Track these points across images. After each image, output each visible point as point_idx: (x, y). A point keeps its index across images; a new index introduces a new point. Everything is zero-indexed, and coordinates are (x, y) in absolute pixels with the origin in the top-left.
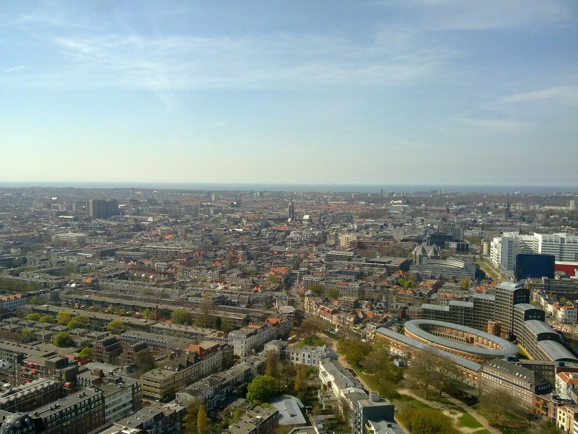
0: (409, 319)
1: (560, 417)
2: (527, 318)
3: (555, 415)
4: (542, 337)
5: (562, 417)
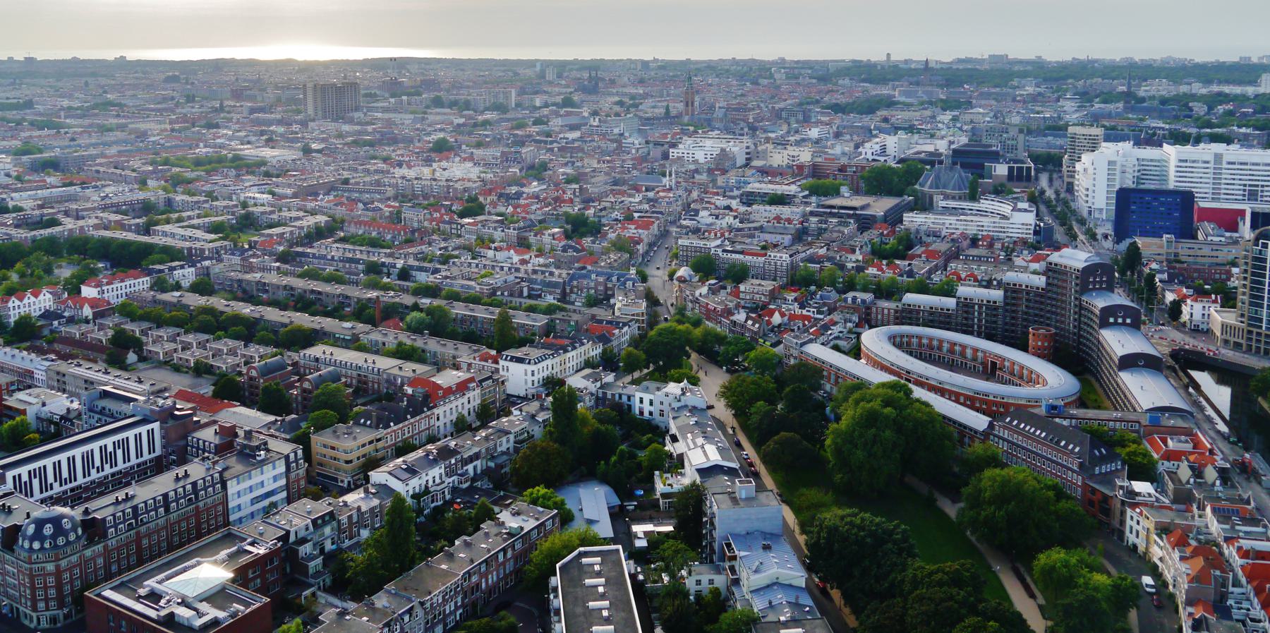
0: (871, 327)
1: (1131, 528)
2: (1104, 324)
3: (1123, 522)
4: (1130, 362)
5: (1136, 527)
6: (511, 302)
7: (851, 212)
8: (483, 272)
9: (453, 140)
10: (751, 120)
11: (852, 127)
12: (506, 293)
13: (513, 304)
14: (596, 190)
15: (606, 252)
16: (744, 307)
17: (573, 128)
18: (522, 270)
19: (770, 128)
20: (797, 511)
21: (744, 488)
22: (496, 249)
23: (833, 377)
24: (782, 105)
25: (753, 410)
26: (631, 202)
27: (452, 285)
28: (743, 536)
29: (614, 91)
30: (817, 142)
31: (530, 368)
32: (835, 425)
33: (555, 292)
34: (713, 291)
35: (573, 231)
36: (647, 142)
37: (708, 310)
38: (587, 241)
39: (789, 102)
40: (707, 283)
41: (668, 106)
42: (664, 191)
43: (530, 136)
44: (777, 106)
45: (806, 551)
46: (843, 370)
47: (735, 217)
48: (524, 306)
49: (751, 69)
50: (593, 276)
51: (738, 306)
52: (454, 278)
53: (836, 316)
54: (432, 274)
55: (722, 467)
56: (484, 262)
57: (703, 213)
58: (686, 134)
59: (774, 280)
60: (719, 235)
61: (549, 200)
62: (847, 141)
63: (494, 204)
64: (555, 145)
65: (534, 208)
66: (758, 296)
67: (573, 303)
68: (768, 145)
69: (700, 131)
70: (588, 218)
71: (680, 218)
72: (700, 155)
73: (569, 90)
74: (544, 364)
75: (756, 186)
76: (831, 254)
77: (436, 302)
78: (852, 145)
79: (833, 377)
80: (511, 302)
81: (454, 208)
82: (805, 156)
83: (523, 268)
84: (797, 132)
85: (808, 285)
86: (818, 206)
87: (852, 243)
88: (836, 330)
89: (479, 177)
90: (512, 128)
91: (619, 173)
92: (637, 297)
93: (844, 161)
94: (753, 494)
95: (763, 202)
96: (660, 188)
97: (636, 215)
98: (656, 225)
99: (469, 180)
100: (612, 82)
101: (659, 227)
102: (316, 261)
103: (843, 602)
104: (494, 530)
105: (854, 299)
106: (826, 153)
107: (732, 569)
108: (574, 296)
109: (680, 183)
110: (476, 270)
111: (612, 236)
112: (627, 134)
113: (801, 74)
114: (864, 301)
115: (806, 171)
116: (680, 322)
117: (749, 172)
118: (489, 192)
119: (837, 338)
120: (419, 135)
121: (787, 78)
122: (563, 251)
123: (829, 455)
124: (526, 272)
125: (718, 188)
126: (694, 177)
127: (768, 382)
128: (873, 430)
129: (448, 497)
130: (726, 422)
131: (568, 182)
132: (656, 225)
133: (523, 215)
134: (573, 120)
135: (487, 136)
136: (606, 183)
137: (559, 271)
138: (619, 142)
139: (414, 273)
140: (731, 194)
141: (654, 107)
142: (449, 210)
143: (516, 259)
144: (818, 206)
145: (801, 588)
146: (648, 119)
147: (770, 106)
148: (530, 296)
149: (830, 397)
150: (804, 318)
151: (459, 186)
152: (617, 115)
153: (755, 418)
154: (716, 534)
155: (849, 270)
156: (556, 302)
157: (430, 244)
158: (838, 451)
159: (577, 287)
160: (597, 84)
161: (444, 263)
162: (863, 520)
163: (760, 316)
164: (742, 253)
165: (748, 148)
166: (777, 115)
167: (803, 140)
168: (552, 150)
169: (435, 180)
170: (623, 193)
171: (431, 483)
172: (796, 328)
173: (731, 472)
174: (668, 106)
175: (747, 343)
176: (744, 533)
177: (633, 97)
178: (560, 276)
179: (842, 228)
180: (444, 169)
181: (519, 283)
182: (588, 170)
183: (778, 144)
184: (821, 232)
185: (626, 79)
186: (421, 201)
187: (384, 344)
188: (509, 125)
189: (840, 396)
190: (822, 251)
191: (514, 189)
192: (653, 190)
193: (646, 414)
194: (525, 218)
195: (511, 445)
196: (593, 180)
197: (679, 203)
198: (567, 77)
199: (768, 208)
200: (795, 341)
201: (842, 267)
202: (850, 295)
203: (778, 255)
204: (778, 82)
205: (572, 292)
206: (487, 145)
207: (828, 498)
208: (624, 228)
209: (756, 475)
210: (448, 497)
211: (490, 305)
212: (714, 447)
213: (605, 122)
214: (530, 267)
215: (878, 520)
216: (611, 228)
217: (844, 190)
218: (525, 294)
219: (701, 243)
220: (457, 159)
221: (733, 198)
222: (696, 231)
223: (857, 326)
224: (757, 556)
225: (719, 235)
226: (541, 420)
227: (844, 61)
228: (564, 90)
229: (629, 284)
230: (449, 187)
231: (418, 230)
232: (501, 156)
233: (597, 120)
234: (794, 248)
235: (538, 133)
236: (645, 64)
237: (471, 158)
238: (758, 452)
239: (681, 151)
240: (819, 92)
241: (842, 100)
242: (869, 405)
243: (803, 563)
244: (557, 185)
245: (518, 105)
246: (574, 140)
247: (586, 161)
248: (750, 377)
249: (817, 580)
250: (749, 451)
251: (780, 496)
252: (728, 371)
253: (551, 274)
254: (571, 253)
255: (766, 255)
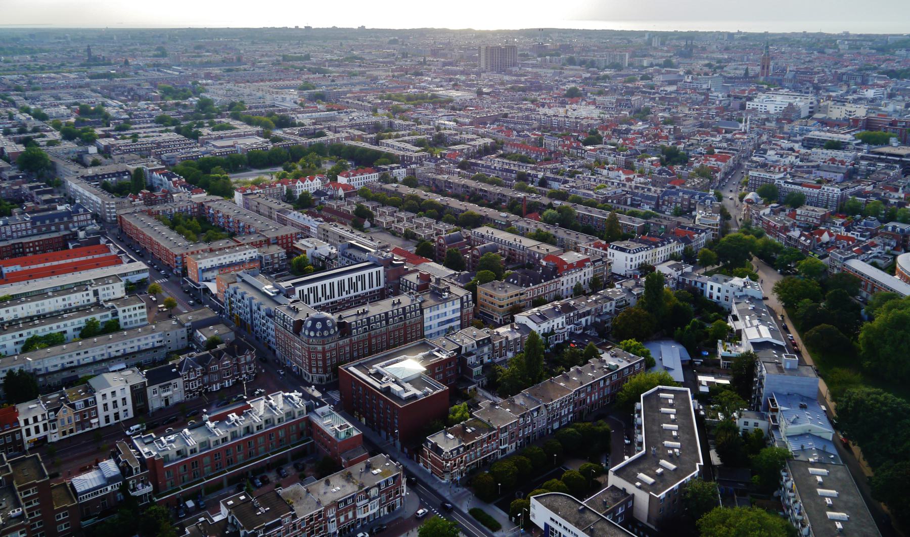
6: (618, 208)
7: (898, 159)
8: (599, 185)
9: (581, 89)
10: (816, 81)
11: (905, 89)
12: (615, 201)
13: (620, 210)
14: (686, 130)
15: (692, 177)
16: (798, 227)
17: (671, 83)
18: (628, 186)
19: (832, 88)
20: (829, 384)
21: (788, 360)
22: (609, 169)
23: (869, 287)
24: (843, 70)
25: (800, 304)
26: (713, 141)
27: (576, 193)
28: (785, 395)
29: (705, 56)
30: (873, 100)
31: (630, 256)
32: (869, 324)
33: (651, 203)
34: (774, 212)
35: (667, 160)
36: (729, 96)
37: (770, 226)
38: (677, 168)
39: (849, 68)
40: (770, 206)
41: (747, 69)
42: (739, 134)
43: (638, 88)
44: (839, 71)
45: (835, 415)
46: (879, 282)
47: (797, 157)
48: (627, 211)
49: (819, 40)
50: (681, 194)
51: (793, 225)
52: (578, 188)
53: (876, 240)
54: (563, 184)
55: (772, 343)
56: (600, 178)
57: (770, 152)
58: (760, 91)
59: (826, 207)
60: (782, 170)
61: (650, 136)
62: (898, 101)
63: (609, 137)
64: (657, 95)
65: (638, 141)
66: (811, 219)
67: (664, 212)
68: (829, 102)
69: (772, 89)
70: (679, 151)
71: (751, 155)
72: (771, 108)
73: (669, 54)
74: (640, 254)
75: (815, 134)
76: (876, 191)
77: (565, 204)
78: (903, 104)
79: (869, 287)
80: (618, 208)
81: (580, 138)
82: (861, 112)
83: (628, 184)
84: (855, 92)
85: (854, 214)
86: (869, 152)
87: (896, 183)
88: (875, 251)
89: (599, 117)
90: (625, 82)
91: (705, 118)
92: (713, 212)
93: (895, 117)
94: (796, 366)
95: (822, 147)
96: (737, 132)
97: (716, 151)
98: (731, 159)
99: (592, 119)
100: (704, 49)
101: (734, 161)
102: (483, 169)
103: (862, 457)
104: (598, 365)
105: (894, 228)
106: (879, 110)
107: (774, 418)
108: (665, 207)
109: (753, 128)
110: (594, 183)
111: (697, 165)
112: (713, 89)
113: (862, 46)
114: (902, 230)
115: (860, 124)
116: (746, 233)
117: (811, 122)
118: (606, 128)
119: (875, 257)
120: (557, 85)
121: (850, 48)
122: (659, 174)
123: (861, 346)
124: (630, 187)
125: (783, 134)
126: (764, 124)
127: (813, 283)
128: (902, 332)
129: (567, 338)
130: (776, 311)
131: (666, 123)
132: (731, 159)
133: (630, 146)
134: (672, 77)
135: (606, 87)
136: (694, 126)
137: (655, 188)
138: (707, 95)
139: (550, 182)
140: (795, 138)
141: (736, 69)
142: (577, 139)
143: (623, 177)
144: (869, 152)
145: (828, 441)
146: (731, 78)
147: (833, 71)
148: (632, 205)
149: (865, 302)
150: (848, 239)
151: (584, 122)
152: (706, 74)
153: (801, 311)
154: (764, 391)
155: (892, 205)
156: (651, 210)
157: (562, 163)
158: (869, 344)
159: (668, 201)
160: (691, 50)
161: (571, 177)
162: (886, 398)
163: (812, 234)
164: (800, 185)
165: (811, 103)
166: (839, 79)
167: (860, 99)
168: (654, 99)
169: (567, 117)
170: (707, 134)
171: (555, 327)
172: (841, 246)
173: (779, 348)
174: (747, 69)
175: (799, 254)
176: (786, 393)
177: (719, 61)
178: (655, 192)
179: (888, 171)
180: (574, 110)
181: (624, 195)
182: (681, 115)
183: (838, 101)
184: (869, 173)
185: (715, 47)
186: (557, 131)
187: (528, 230)
188: (622, 79)
189: (875, 302)
190: (869, 188)
191: (624, 127)
192: (731, 132)
193: (715, 298)
194: (630, 148)
195: (613, 308)
196: (685, 123)
197: (752, 143)
198: (669, 44)
199: (825, 151)
200: (840, 256)
201: (886, 202)
202: (890, 225)
203: (831, 188)
204: (842, 52)
205: (663, 204)
206: (606, 94)
207: (858, 377)
208: (706, 160)
209: (798, 353)
210: (567, 338)
211: (603, 209)
212: (766, 328)
213: (697, 79)
214: (633, 184)
215: (899, 400)
216: (696, 159)
217: (893, 141)
218: (629, 203)
219: (768, 175)
220: (584, 103)
221: (796, 142)
222: (764, 166)
223: (894, 249)
224: (795, 412)
225: (782, 170)
226: (635, 293)
227: (902, 35)
228: (666, 54)
229: (708, 202)
230: (577, 123)
231: (554, 152)
232: (616, 102)
233: (690, 77)
234: (845, 184)
235: (644, 86)
236: (731, 36)
237: (594, 103)
238: (801, 336)
239: (755, 104)
240: (878, 60)
241: (897, 67)
242: (900, 312)
243: (831, 422)
244: (657, 125)
245: (630, 65)
246: (671, 93)
247: (680, 108)
248: (799, 280)
249: (841, 437)
250: (794, 334)
251: (817, 370)
252: (781, 273)
253: (649, 190)
254: (664, 176)
255: (820, 188)
